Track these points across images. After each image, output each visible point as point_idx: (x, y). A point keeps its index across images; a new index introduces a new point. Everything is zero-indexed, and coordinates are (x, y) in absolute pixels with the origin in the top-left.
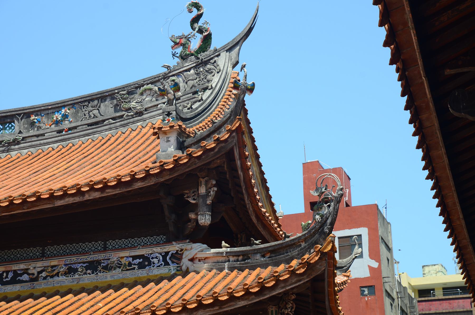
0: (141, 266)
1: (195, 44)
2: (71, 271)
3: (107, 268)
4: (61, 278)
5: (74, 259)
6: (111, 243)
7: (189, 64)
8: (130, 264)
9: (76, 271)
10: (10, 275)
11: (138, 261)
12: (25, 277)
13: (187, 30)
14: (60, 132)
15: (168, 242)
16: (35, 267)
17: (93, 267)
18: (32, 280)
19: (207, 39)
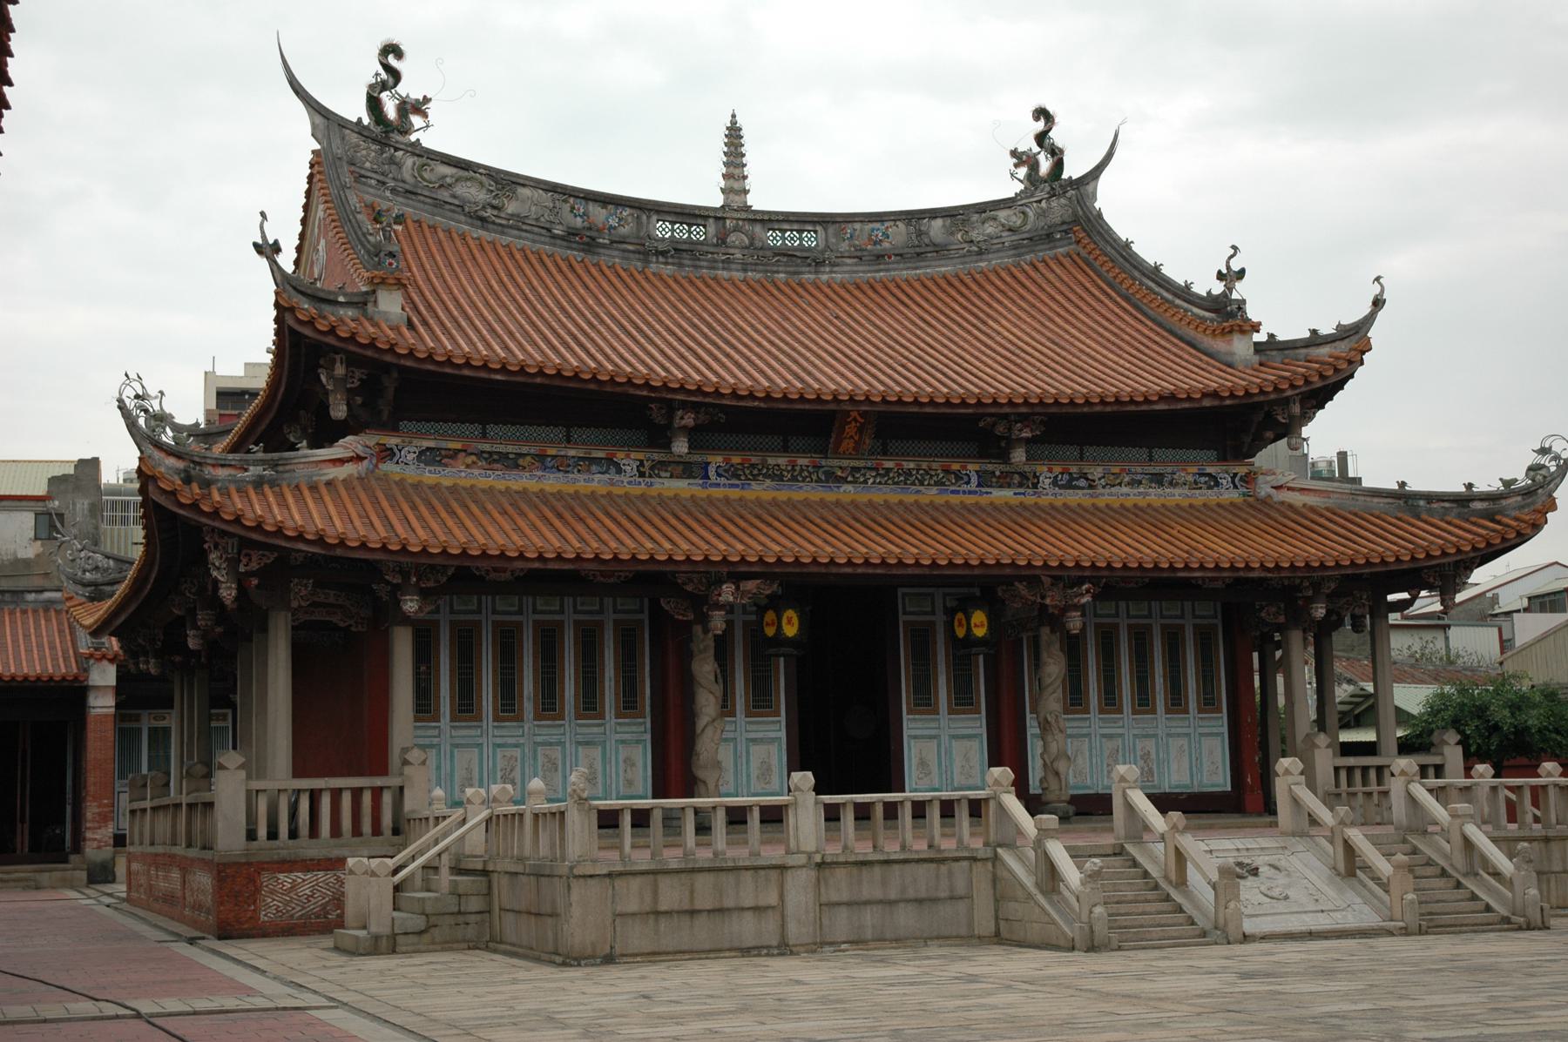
0: (1210, 488)
1: (1045, 165)
2: (1135, 483)
3: (1172, 484)
4: (1125, 490)
5: (1139, 469)
6: (1158, 453)
7: (1039, 195)
8: (1196, 482)
9: (1140, 483)
10: (1066, 477)
11: (1203, 479)
12: (1082, 483)
13: (1036, 149)
14: (879, 257)
15: (1223, 458)
16: (1096, 472)
17: (1158, 479)
18: (1091, 487)
19: (1058, 166)
